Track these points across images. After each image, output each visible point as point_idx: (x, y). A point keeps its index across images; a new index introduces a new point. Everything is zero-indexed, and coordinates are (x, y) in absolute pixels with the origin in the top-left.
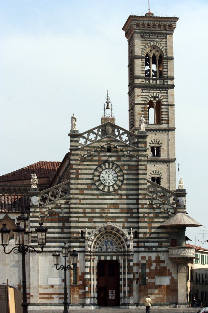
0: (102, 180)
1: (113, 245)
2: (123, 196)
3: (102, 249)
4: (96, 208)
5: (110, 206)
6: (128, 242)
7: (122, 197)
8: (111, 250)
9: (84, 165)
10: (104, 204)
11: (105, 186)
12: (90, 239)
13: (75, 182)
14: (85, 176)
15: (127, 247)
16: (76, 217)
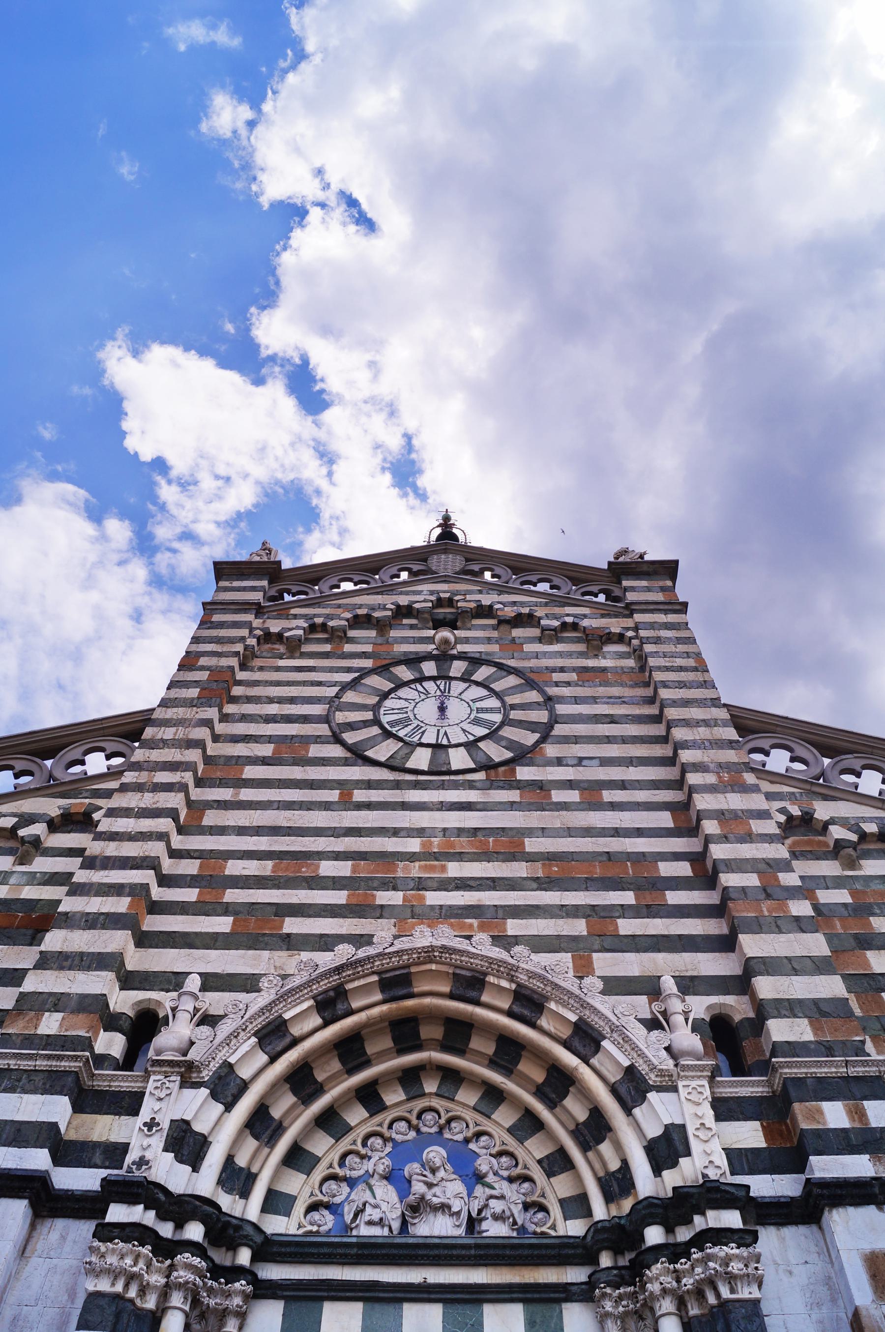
0: (392, 723)
1: (479, 1178)
2: (553, 792)
3: (348, 1218)
4: (321, 855)
5: (452, 845)
6: (652, 1096)
7: (550, 797)
8: (461, 1231)
9: (278, 669)
10: (395, 832)
11: (410, 747)
12: (214, 1066)
13: (188, 716)
14: (273, 709)
15: (657, 1170)
16: (117, 890)
